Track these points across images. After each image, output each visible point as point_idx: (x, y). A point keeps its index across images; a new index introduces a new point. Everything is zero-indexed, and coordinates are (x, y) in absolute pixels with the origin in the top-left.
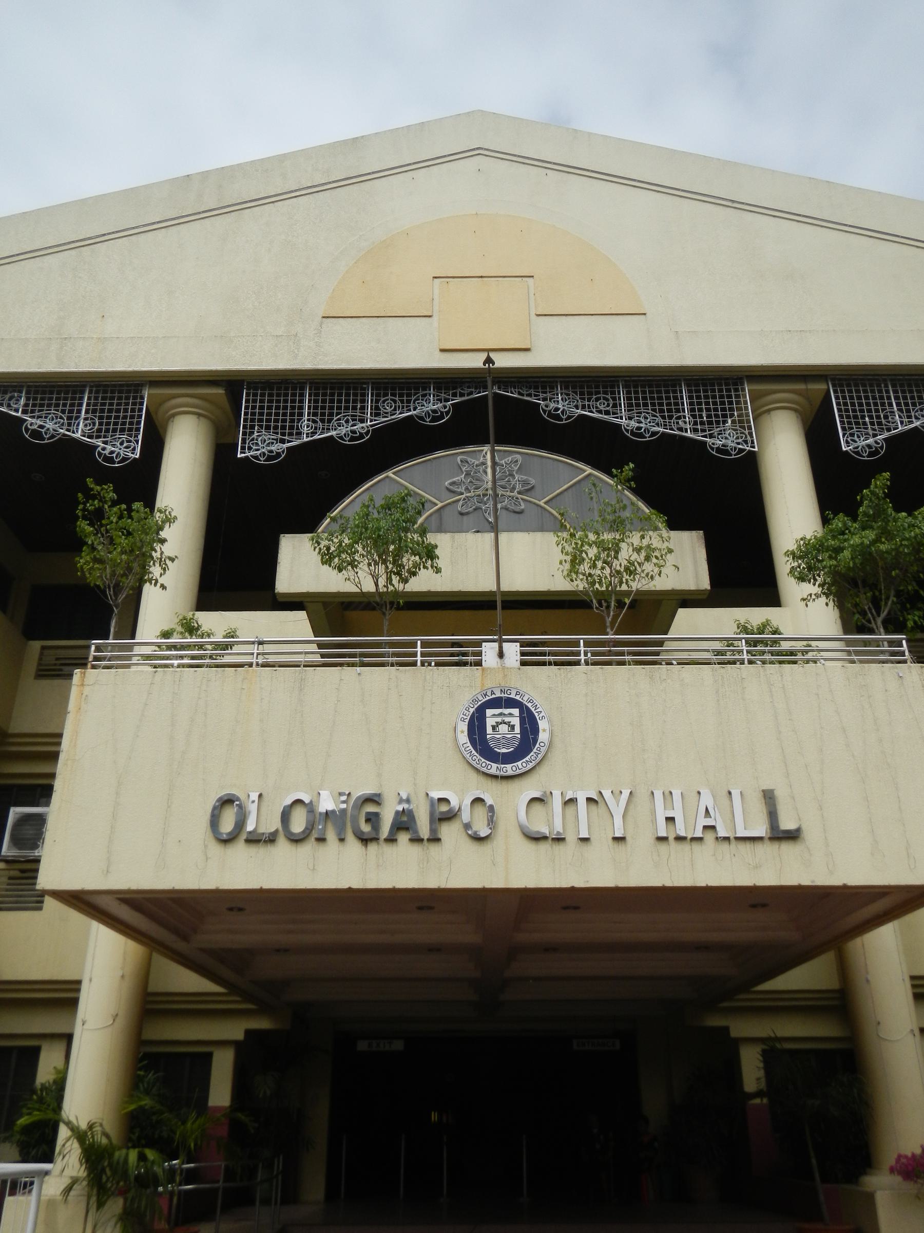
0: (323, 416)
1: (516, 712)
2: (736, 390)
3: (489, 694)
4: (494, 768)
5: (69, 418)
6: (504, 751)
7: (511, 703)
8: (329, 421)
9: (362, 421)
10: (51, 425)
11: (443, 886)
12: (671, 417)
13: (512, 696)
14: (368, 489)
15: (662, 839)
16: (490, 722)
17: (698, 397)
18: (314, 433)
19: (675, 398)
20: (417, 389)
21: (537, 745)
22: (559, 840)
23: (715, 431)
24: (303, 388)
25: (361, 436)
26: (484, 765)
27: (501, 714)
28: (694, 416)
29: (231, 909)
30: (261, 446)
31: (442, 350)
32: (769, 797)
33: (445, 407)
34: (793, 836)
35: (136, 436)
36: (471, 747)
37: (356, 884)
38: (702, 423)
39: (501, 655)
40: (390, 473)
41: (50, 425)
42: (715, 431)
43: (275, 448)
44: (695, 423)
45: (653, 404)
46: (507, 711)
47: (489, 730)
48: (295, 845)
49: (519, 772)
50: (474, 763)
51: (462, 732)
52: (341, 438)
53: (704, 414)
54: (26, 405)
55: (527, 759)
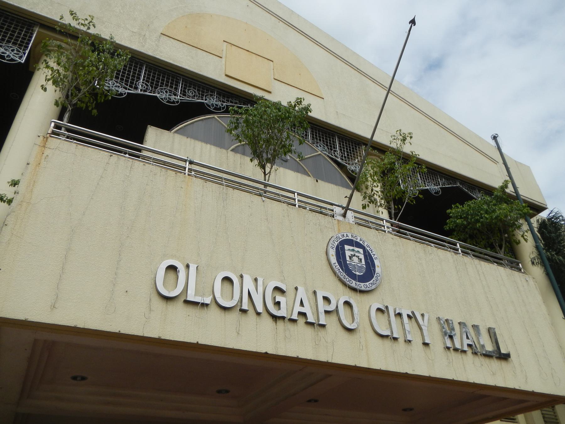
1: (361, 251)
2: (359, 148)
3: (345, 235)
4: (354, 284)
6: (357, 273)
7: (358, 245)
8: (156, 88)
9: (175, 95)
11: (330, 361)
12: (331, 150)
13: (358, 240)
14: (202, 120)
15: (448, 348)
16: (348, 254)
17: (343, 145)
18: (145, 91)
19: (333, 142)
20: (208, 90)
21: (376, 275)
22: (395, 339)
23: (351, 162)
24: (142, 65)
25: (173, 102)
26: (348, 280)
27: (353, 250)
28: (342, 153)
29: (75, 378)
31: (227, 75)
32: (491, 332)
33: (222, 105)
34: (505, 357)
35: (24, 50)
36: (338, 267)
37: (271, 351)
38: (345, 157)
39: (344, 215)
40: (216, 116)
42: (351, 162)
43: (121, 90)
44: (342, 156)
45: (323, 141)
46: (356, 249)
47: (348, 258)
48: (223, 312)
49: (368, 289)
50: (342, 277)
51: (333, 255)
52: (162, 99)
53: (346, 153)
55: (371, 281)
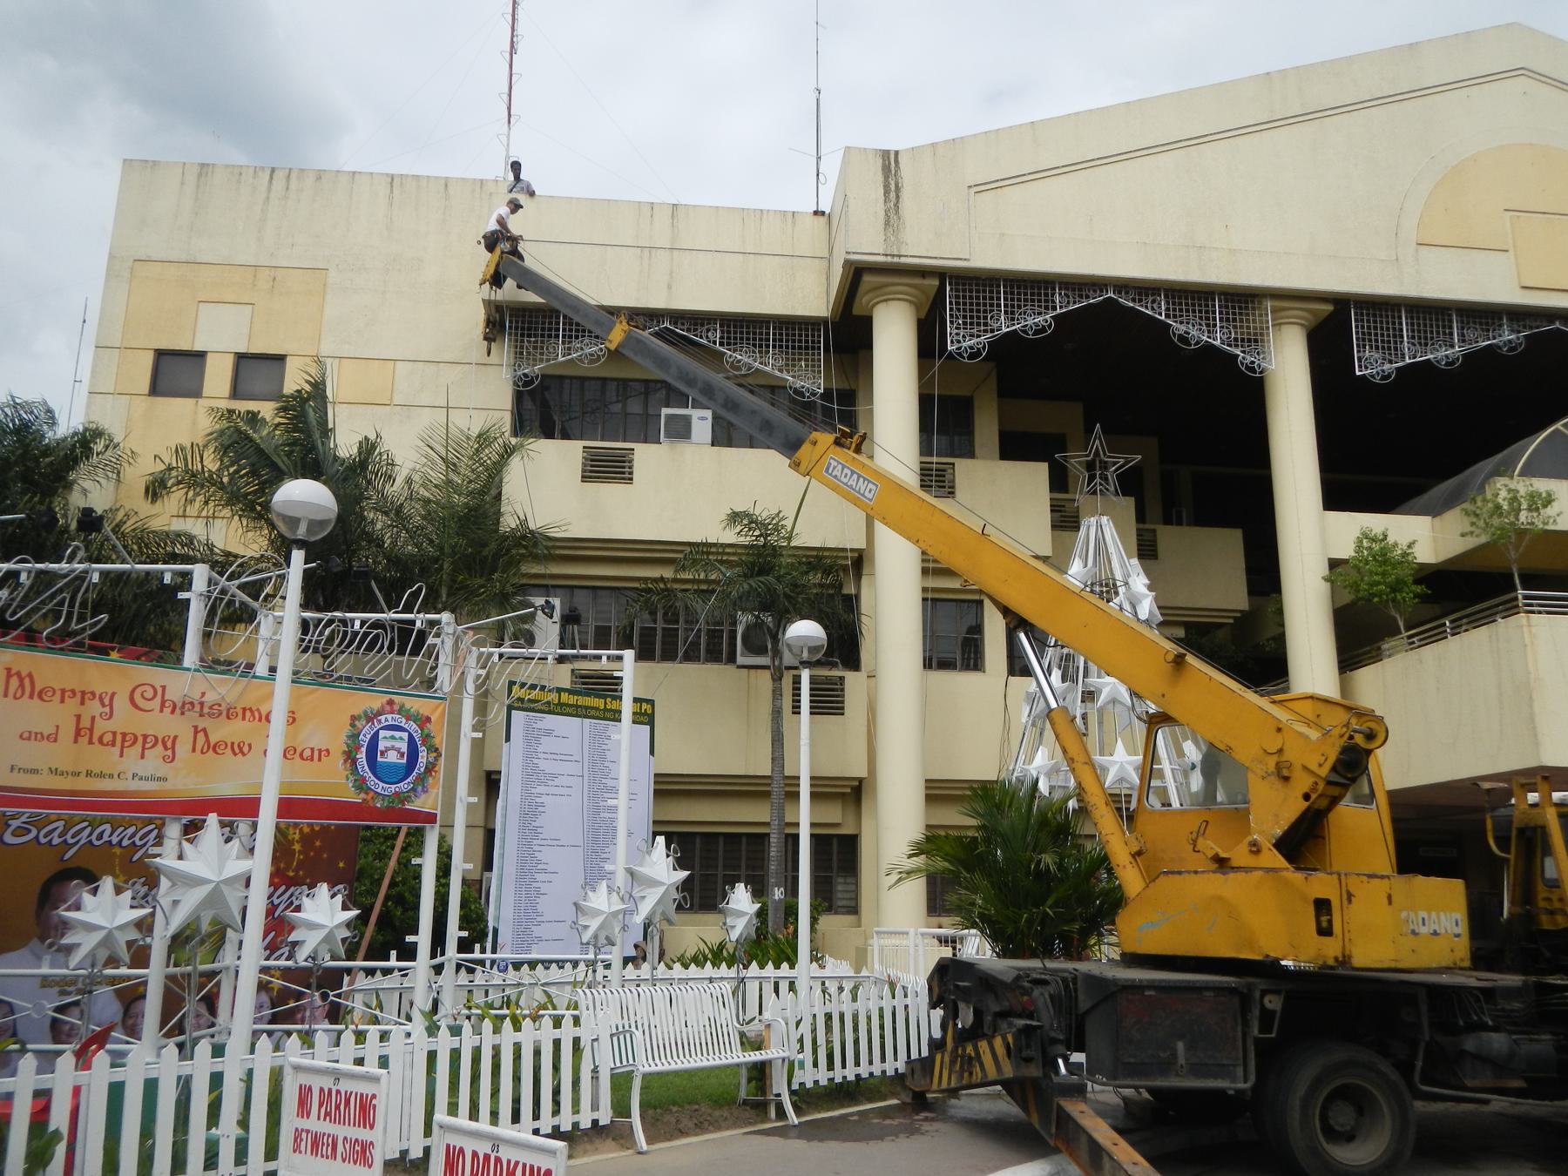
0: (1422, 340)
5: (1208, 325)
9: (1452, 346)
10: (1198, 334)
30: (1371, 364)
40: (1559, 425)
41: (1194, 332)
43: (1387, 367)
54: (1167, 309)
